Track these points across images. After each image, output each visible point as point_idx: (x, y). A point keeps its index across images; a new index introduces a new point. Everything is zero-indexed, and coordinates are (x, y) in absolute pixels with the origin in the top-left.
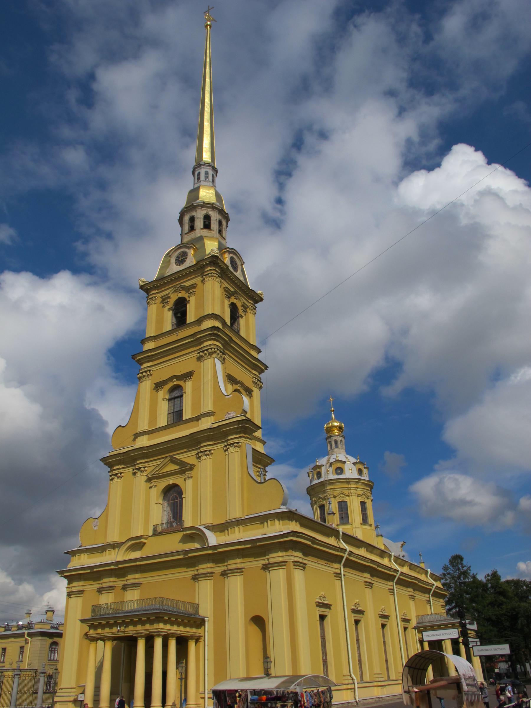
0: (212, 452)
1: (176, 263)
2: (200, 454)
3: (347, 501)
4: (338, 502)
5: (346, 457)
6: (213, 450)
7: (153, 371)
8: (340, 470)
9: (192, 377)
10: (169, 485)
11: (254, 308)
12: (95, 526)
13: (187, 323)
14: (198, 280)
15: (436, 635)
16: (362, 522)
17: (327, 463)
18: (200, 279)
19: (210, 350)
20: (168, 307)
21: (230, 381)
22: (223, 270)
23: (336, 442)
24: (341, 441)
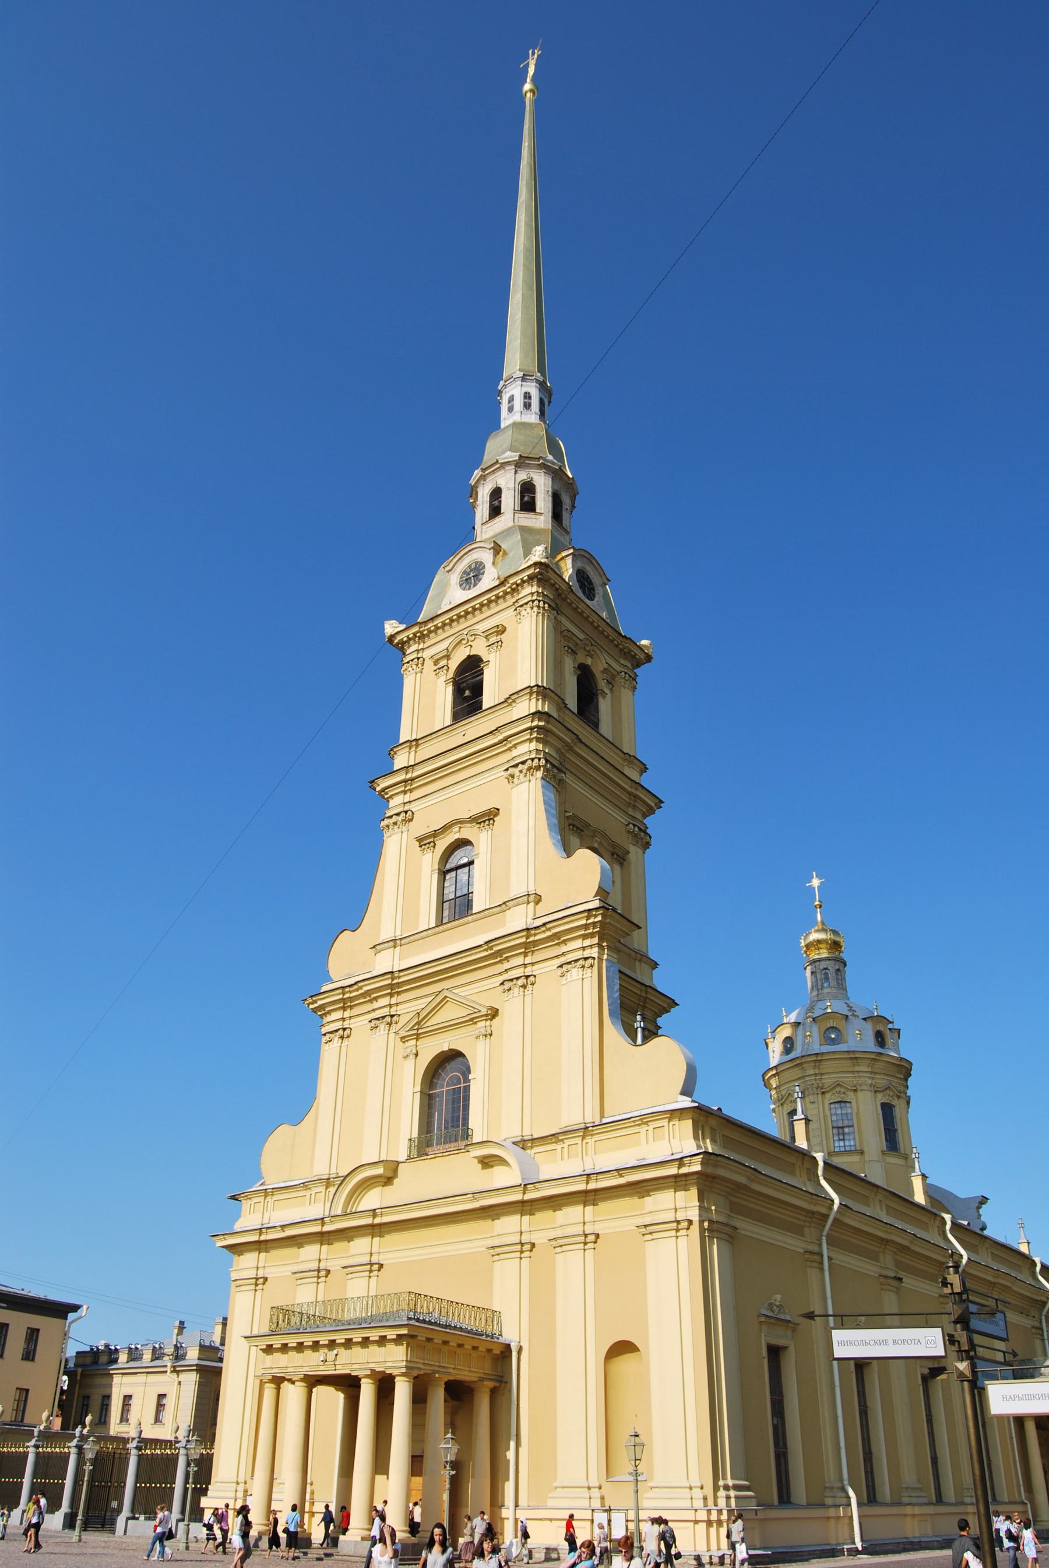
0: (532, 979)
2: (507, 985)
6: (535, 976)
9: (491, 822)
11: (633, 676)
14: (504, 616)
15: (872, 1343)
16: (885, 1149)
19: (529, 762)
20: (443, 678)
21: (575, 829)
24: (838, 970)
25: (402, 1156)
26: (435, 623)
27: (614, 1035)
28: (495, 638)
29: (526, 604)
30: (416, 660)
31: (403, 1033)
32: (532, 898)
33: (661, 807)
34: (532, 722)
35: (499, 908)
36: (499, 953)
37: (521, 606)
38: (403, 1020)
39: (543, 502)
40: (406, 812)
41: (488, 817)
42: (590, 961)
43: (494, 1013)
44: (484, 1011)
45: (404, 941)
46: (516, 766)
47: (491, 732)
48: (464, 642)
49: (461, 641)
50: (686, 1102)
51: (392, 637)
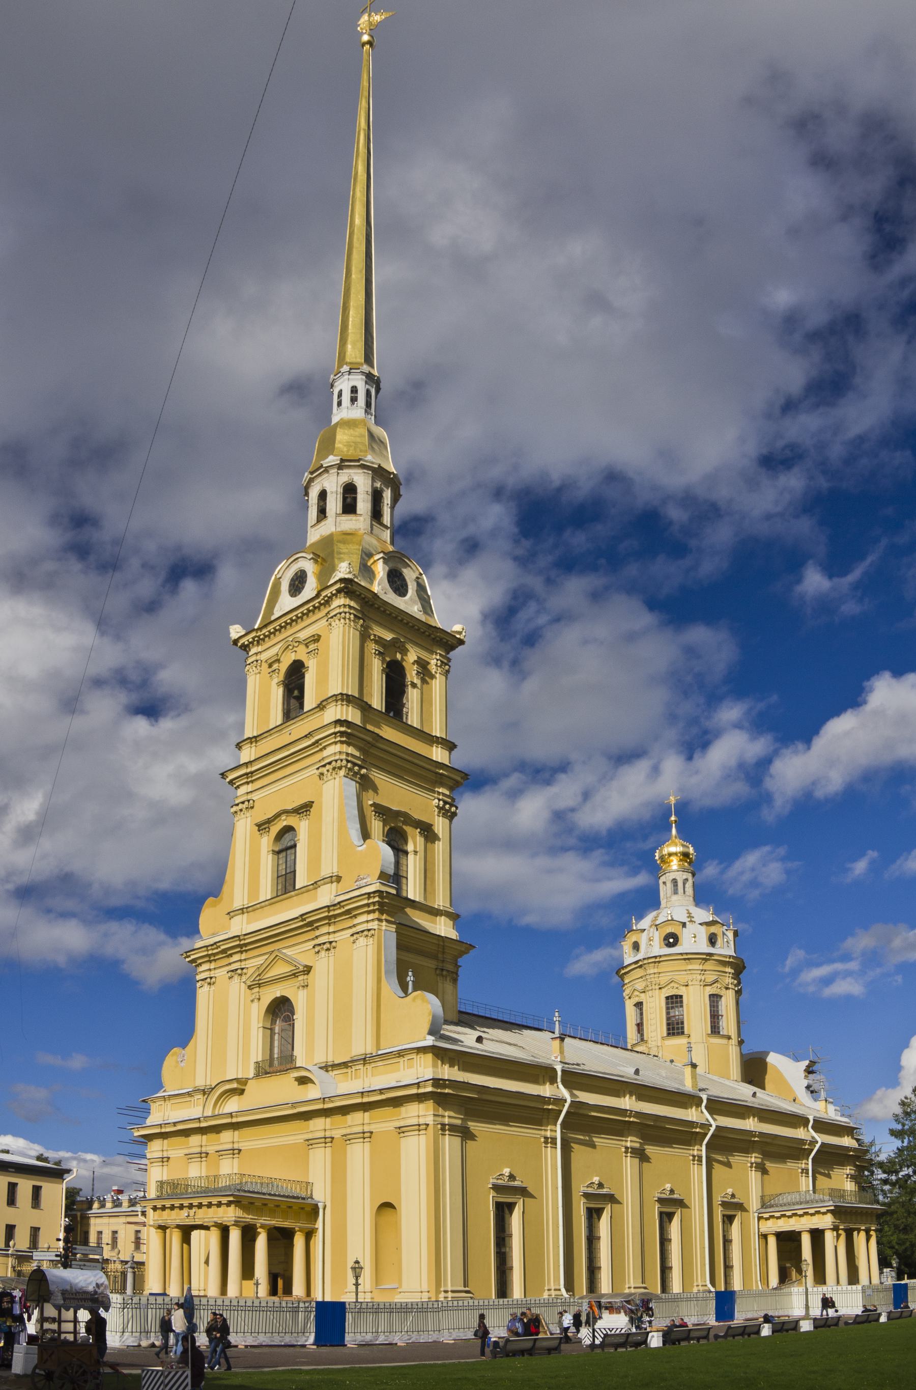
0: (334, 944)
1: (290, 592)
2: (317, 949)
3: (681, 997)
4: (667, 998)
5: (689, 913)
6: (336, 942)
7: (254, 801)
8: (672, 940)
10: (277, 998)
12: (181, 1061)
13: (306, 709)
17: (651, 926)
18: (323, 622)
19: (334, 763)
20: (276, 680)
22: (366, 602)
23: (675, 882)
25: (251, 1075)
26: (269, 629)
27: (390, 988)
28: (313, 646)
29: (335, 615)
30: (255, 663)
31: (249, 983)
32: (334, 878)
33: (468, 779)
34: (335, 728)
35: (312, 886)
36: (310, 924)
37: (332, 617)
38: (250, 971)
39: (364, 504)
40: (249, 801)
41: (304, 809)
42: (372, 932)
43: (308, 970)
44: (301, 968)
45: (249, 909)
46: (324, 766)
47: (306, 736)
48: (290, 647)
49: (287, 647)
50: (430, 1041)
51: (235, 642)
